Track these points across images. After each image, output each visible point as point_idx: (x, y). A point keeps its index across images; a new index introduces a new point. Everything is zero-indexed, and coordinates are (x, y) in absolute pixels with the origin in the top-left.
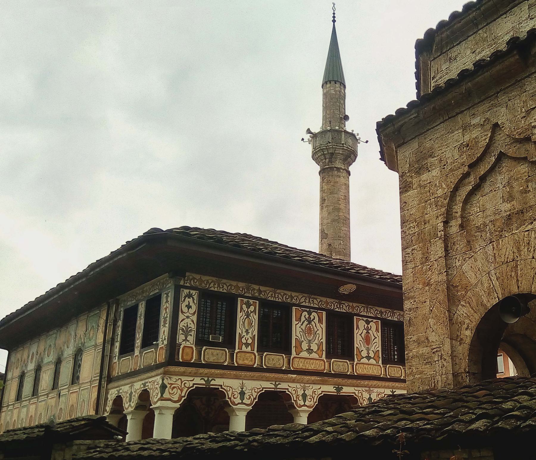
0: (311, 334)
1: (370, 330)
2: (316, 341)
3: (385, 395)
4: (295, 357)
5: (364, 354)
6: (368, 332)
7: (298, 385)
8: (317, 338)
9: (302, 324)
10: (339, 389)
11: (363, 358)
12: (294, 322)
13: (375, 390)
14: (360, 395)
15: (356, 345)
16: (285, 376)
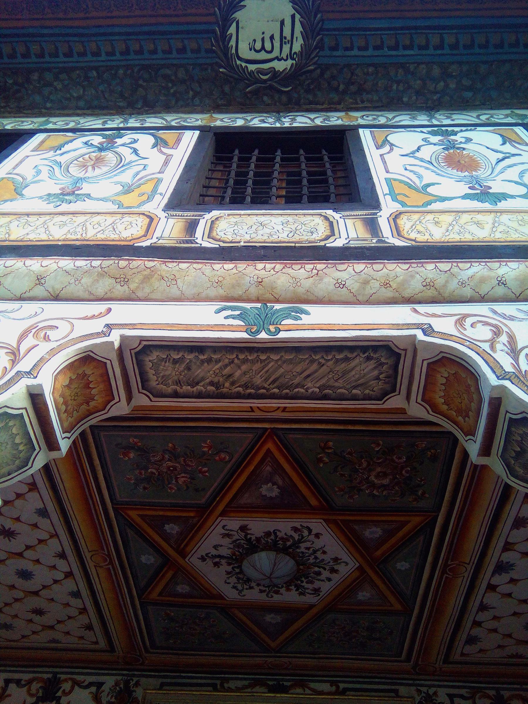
9: (62, 154)
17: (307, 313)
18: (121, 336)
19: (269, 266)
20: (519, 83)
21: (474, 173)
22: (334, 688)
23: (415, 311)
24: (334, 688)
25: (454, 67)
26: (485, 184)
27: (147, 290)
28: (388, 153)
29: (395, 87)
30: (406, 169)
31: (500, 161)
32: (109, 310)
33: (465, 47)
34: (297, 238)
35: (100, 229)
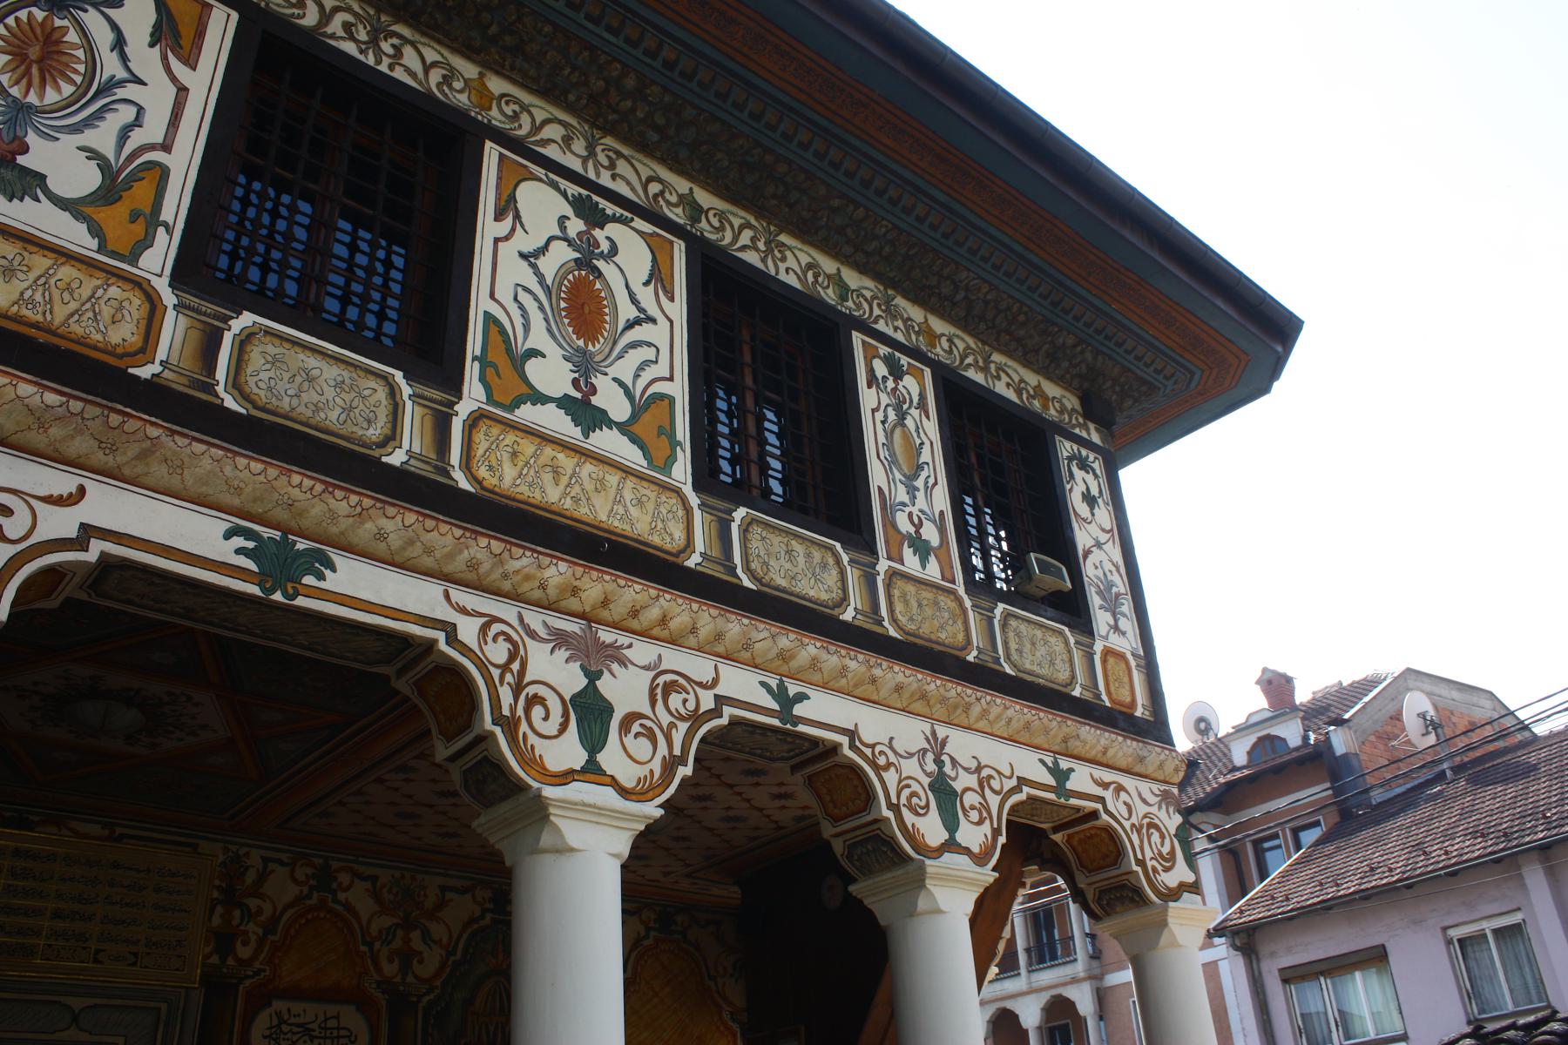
3: (719, 699)
10: (280, 563)
11: (539, 399)
13: (643, 652)
14: (497, 652)
15: (480, 304)
17: (334, 570)
18: (102, 553)
19: (307, 483)
20: (719, 155)
21: (590, 347)
22: (107, 832)
23: (447, 596)
24: (107, 832)
25: (656, 89)
26: (594, 380)
27: (140, 469)
28: (507, 238)
29: (567, 71)
30: (516, 299)
31: (630, 325)
32: (82, 491)
33: (682, 74)
34: (348, 429)
35: (73, 306)
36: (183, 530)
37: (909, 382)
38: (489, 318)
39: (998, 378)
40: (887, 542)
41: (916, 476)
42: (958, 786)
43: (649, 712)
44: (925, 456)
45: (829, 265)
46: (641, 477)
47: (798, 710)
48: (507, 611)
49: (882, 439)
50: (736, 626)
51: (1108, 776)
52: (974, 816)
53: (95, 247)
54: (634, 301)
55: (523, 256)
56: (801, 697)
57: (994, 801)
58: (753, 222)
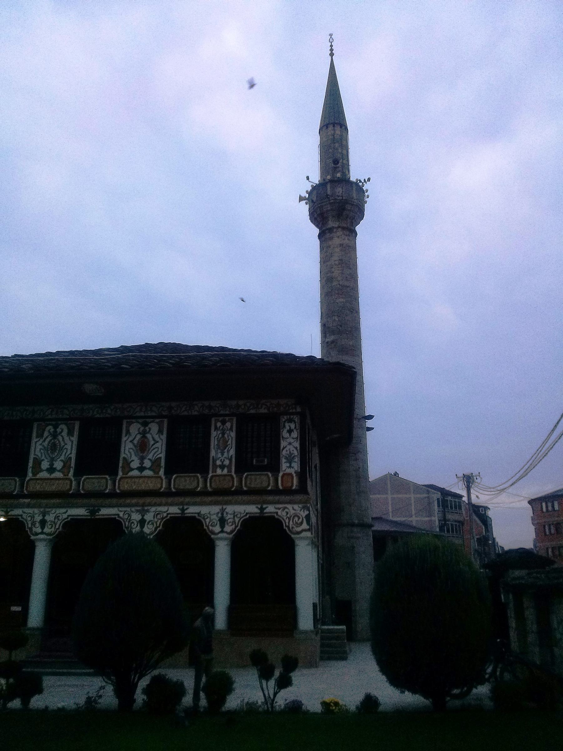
0: (55, 451)
1: (147, 433)
2: (62, 458)
3: (168, 514)
4: (31, 479)
5: (135, 464)
6: (144, 437)
7: (36, 511)
8: (64, 453)
9: (44, 441)
10: (93, 512)
11: (133, 470)
12: (34, 440)
13: (153, 509)
14: (126, 517)
15: (122, 455)
16: (16, 502)
32: (67, 511)
36: (80, 512)
37: (228, 425)
38: (124, 458)
39: (262, 407)
40: (213, 469)
41: (225, 448)
42: (227, 518)
43: (152, 519)
44: (229, 442)
45: (207, 403)
46: (152, 477)
47: (186, 512)
48: (128, 509)
49: (216, 443)
50: (170, 500)
51: (280, 506)
52: (231, 524)
53: (62, 475)
54: (154, 439)
55: (131, 442)
56: (187, 509)
57: (237, 520)
58: (186, 403)
